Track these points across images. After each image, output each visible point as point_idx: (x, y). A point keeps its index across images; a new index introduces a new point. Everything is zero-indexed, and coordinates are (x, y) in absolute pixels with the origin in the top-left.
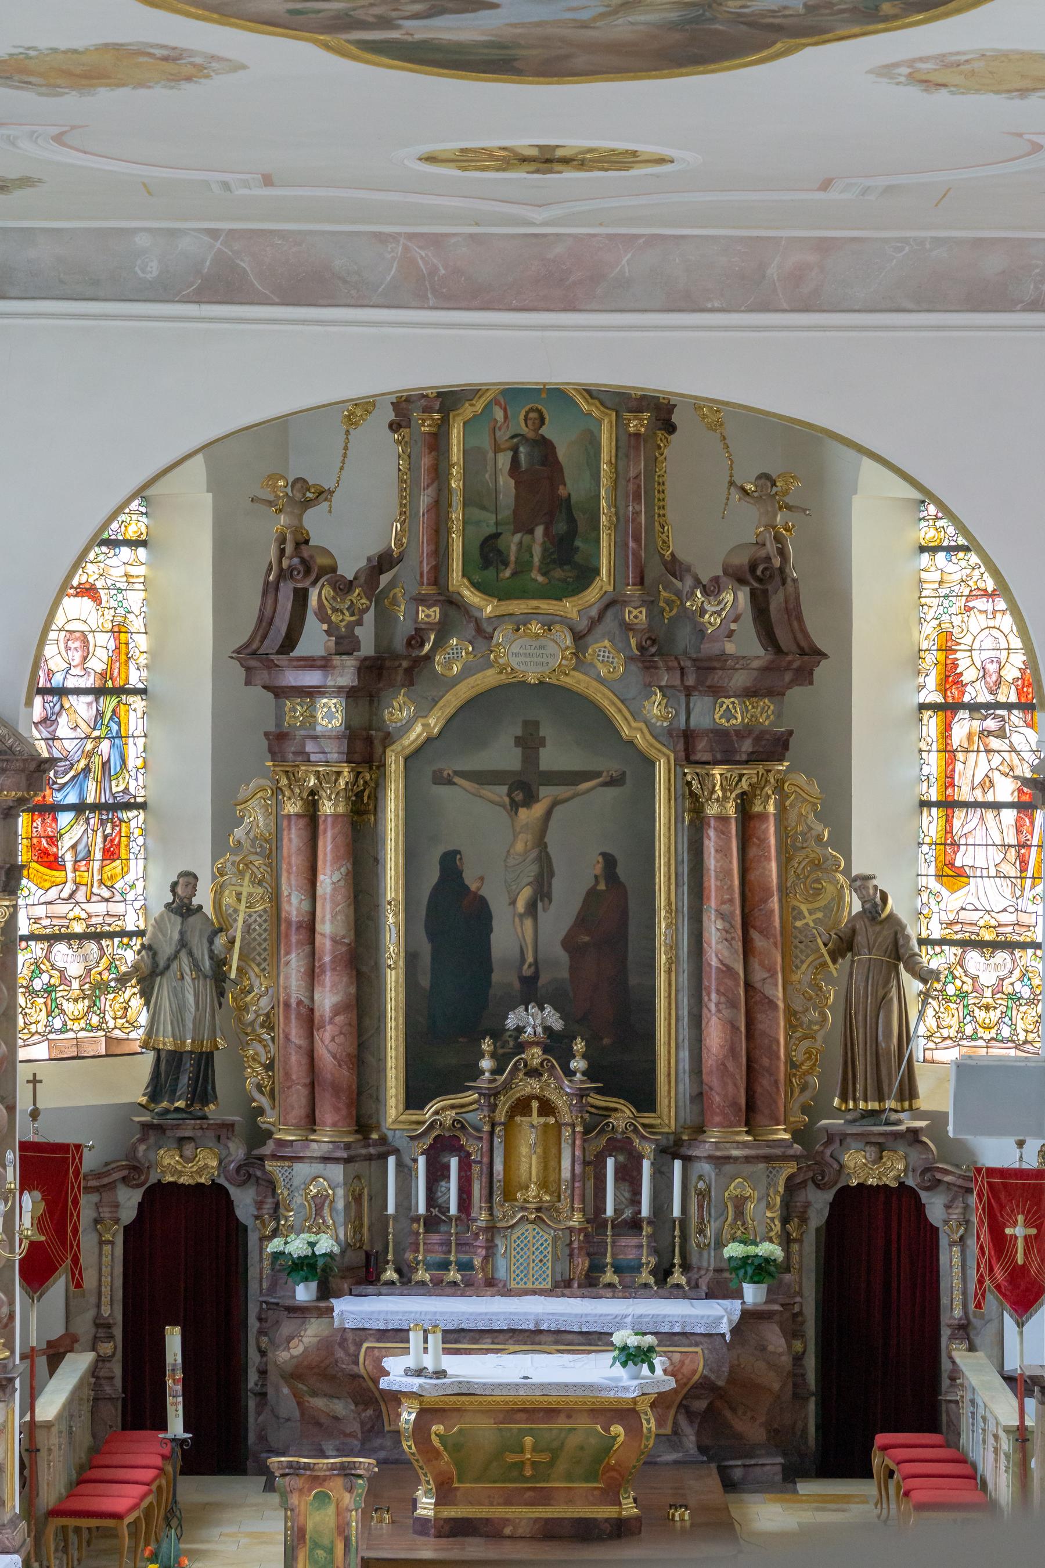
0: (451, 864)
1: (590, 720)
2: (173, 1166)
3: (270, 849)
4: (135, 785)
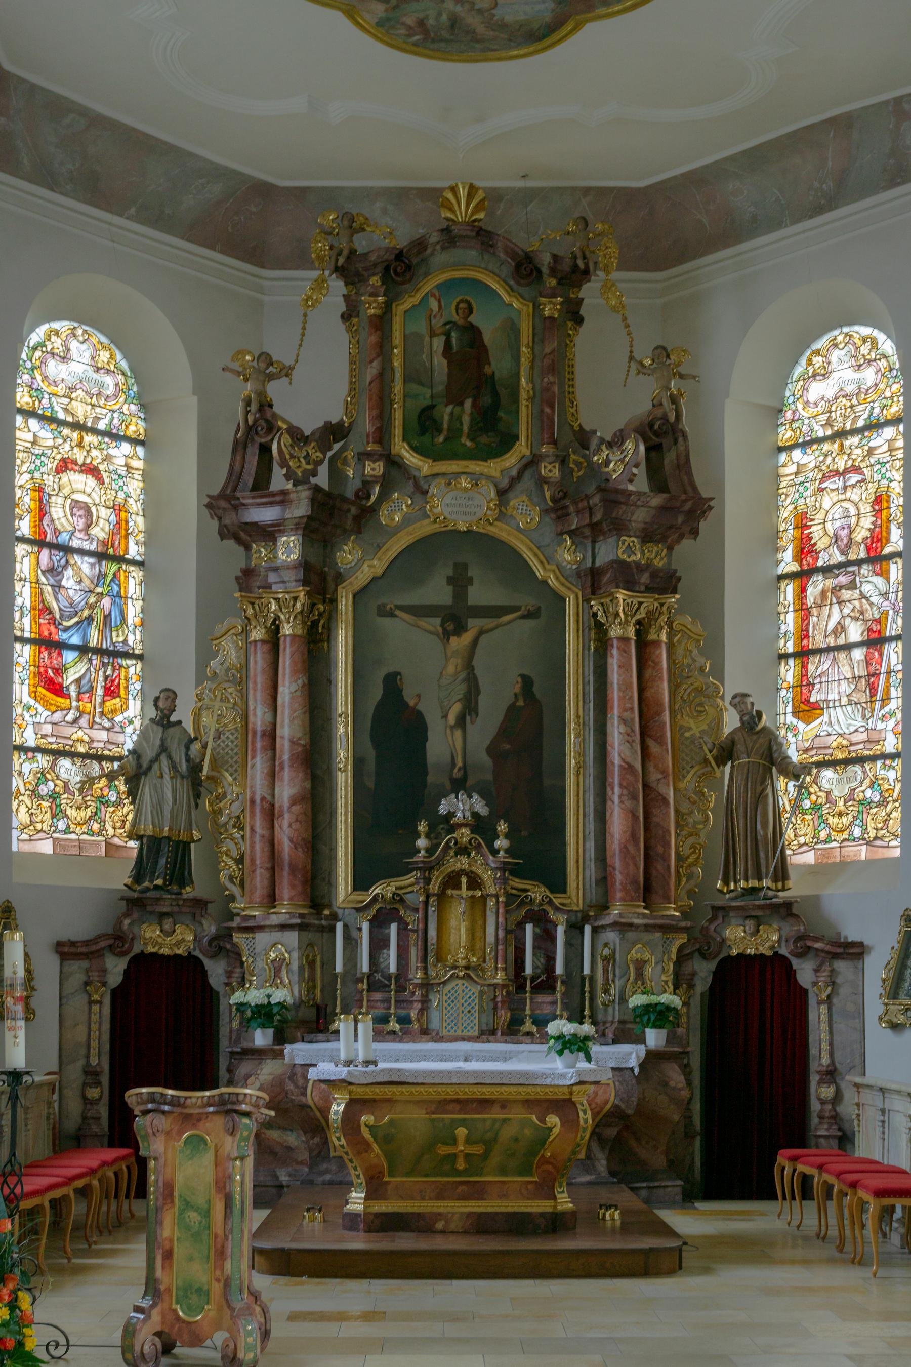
0: (392, 682)
1: (512, 566)
3: (240, 677)
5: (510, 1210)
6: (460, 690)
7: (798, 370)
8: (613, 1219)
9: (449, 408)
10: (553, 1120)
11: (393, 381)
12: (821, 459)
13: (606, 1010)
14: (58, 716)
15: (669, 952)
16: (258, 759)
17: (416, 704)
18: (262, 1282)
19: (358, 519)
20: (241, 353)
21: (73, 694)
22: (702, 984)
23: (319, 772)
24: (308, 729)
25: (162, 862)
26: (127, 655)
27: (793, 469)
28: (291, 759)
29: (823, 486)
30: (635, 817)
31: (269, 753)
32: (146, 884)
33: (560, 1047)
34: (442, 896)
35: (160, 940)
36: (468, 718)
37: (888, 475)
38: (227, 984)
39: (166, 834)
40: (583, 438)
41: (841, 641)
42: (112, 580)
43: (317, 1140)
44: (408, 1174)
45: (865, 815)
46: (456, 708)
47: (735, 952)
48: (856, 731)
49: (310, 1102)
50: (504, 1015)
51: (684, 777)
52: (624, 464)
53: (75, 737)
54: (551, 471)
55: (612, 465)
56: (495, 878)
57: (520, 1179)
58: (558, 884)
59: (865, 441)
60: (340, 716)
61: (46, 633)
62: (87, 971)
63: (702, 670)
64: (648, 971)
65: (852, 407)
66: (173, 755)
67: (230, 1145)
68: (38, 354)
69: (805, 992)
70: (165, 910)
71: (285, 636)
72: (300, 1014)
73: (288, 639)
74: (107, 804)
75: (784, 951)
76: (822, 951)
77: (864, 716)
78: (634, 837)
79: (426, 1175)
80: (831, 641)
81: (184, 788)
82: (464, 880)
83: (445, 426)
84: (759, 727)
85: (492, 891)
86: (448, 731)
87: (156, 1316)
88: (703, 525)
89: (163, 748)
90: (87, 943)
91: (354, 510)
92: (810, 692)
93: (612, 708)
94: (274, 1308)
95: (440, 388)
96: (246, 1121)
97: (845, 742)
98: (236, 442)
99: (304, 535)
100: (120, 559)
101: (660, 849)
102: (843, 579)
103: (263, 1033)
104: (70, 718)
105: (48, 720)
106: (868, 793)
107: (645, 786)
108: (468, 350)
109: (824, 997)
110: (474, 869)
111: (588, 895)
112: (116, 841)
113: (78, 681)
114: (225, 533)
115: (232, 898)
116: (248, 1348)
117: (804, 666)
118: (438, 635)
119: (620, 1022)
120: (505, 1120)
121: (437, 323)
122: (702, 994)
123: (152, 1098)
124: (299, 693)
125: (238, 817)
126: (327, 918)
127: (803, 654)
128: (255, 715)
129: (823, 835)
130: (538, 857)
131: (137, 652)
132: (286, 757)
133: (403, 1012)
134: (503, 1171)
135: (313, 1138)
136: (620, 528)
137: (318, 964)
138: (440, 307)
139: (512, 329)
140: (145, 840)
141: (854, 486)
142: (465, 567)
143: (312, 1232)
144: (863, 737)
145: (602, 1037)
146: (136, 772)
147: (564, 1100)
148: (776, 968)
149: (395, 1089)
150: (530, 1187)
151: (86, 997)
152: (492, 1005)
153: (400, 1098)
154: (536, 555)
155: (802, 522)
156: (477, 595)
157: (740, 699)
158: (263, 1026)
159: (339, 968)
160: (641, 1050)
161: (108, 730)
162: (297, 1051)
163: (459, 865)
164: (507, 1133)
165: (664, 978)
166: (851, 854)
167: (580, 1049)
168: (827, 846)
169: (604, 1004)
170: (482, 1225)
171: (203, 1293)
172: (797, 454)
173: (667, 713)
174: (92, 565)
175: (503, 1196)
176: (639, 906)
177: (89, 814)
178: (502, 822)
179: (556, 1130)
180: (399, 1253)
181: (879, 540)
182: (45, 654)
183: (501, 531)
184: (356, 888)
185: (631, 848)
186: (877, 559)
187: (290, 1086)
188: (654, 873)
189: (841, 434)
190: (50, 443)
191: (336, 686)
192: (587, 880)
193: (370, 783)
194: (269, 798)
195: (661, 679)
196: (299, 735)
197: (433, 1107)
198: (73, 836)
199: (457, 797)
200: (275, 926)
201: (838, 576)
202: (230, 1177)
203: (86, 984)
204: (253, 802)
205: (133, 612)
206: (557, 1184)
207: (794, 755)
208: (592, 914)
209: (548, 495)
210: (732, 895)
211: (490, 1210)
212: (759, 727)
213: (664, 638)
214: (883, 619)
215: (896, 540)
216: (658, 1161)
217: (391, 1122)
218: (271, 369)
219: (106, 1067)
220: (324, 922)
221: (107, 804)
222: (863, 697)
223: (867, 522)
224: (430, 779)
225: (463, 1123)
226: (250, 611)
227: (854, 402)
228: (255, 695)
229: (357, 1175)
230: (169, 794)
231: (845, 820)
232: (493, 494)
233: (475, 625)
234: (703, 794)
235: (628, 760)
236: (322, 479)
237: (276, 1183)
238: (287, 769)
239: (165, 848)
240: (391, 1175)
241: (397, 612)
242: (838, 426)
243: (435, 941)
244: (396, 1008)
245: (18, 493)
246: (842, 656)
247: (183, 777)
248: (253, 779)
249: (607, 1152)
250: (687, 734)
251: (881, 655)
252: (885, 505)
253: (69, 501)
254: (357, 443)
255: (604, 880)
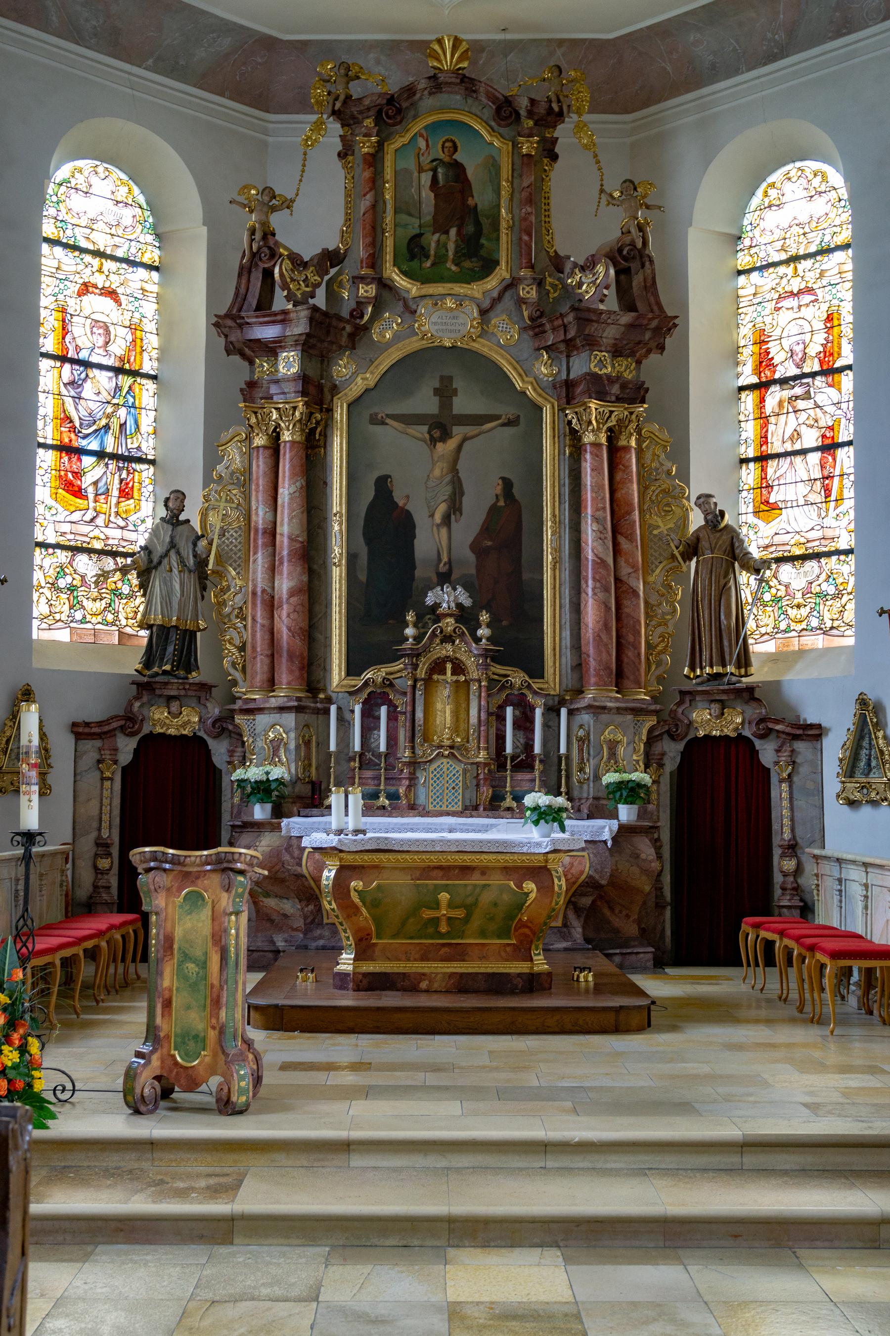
0: (383, 485)
2: (162, 720)
4: (148, 447)
5: (489, 970)
6: (446, 491)
7: (755, 202)
8: (587, 981)
9: (437, 235)
10: (530, 886)
11: (384, 212)
12: (777, 281)
13: (581, 787)
14: (76, 516)
15: (640, 734)
16: (260, 554)
17: (405, 504)
18: (257, 1035)
19: (352, 336)
20: (247, 187)
21: (91, 497)
22: (671, 764)
23: (315, 567)
24: (305, 526)
25: (170, 649)
26: (140, 460)
27: (752, 290)
28: (289, 555)
29: (779, 305)
30: (607, 608)
31: (270, 549)
32: (156, 669)
33: (535, 818)
34: (428, 681)
35: (167, 721)
36: (453, 517)
37: (839, 295)
38: (229, 763)
39: (174, 624)
40: (558, 263)
41: (797, 446)
42: (128, 392)
43: (311, 907)
44: (394, 936)
45: (822, 607)
46: (442, 508)
47: (701, 733)
48: (813, 529)
49: (305, 872)
50: (487, 792)
51: (653, 571)
52: (595, 285)
53: (91, 535)
54: (528, 292)
55: (584, 287)
56: (478, 665)
57: (498, 941)
58: (536, 670)
59: (817, 265)
60: (335, 515)
61: (66, 440)
62: (100, 749)
63: (669, 473)
64: (621, 751)
65: (804, 234)
66: (182, 551)
67: (225, 901)
68: (63, 189)
69: (766, 772)
70: (173, 693)
71: (285, 442)
72: (296, 790)
73: (288, 445)
74: (120, 596)
75: (747, 733)
76: (783, 732)
77: (819, 515)
78: (606, 626)
79: (411, 938)
80: (789, 447)
81: (192, 581)
82: (449, 666)
83: (432, 253)
84: (722, 525)
85: (475, 675)
86: (435, 528)
87: (155, 1061)
88: (668, 341)
89: (173, 545)
90: (100, 724)
91: (349, 328)
92: (769, 493)
93: (586, 508)
94: (267, 1059)
95: (428, 218)
96: (241, 878)
97: (803, 540)
98: (242, 268)
99: (303, 351)
100: (135, 373)
101: (631, 638)
102: (798, 391)
103: (263, 809)
104: (88, 517)
105: (68, 519)
106: (824, 586)
107: (617, 580)
108: (453, 186)
109: (785, 775)
110: (458, 655)
111: (564, 680)
112: (128, 630)
113: (95, 483)
114: (231, 349)
115: (234, 683)
116: (241, 1092)
117: (764, 470)
118: (424, 441)
119: (594, 798)
120: (485, 886)
121: (425, 160)
122: (671, 773)
123: (154, 857)
124: (297, 494)
125: (241, 608)
126: (322, 701)
127: (762, 459)
128: (257, 514)
129: (783, 626)
130: (518, 645)
131: (149, 457)
132: (285, 553)
133: (392, 789)
134: (483, 934)
135: (307, 906)
136: (592, 343)
137: (314, 744)
138: (428, 146)
139: (493, 166)
140: (155, 629)
141: (807, 305)
142: (450, 379)
143: (305, 990)
144: (819, 534)
145: (578, 814)
146: (147, 566)
147: (540, 868)
148: (740, 748)
149: (382, 856)
150: (508, 949)
151: (98, 773)
152: (475, 783)
153: (387, 865)
154: (515, 369)
155: (761, 340)
156: (462, 405)
157: (704, 500)
158: (262, 801)
159: (333, 747)
160: (614, 825)
161: (122, 528)
162: (293, 825)
163: (444, 652)
164: (486, 898)
165: (635, 758)
166: (809, 643)
167: (554, 820)
168: (787, 635)
169: (579, 782)
170: (463, 985)
171: (200, 1040)
172: (755, 275)
173: (637, 512)
174: (110, 378)
175: (483, 958)
176: (611, 691)
177: (104, 605)
178: (484, 612)
179: (533, 896)
180: (386, 1009)
181: (831, 354)
182: (66, 459)
183: (482, 347)
184: (348, 674)
185: (604, 637)
186: (829, 372)
187: (286, 857)
188: (626, 660)
189: (795, 259)
190: (73, 268)
191: (332, 488)
192: (563, 666)
193: (363, 577)
194: (269, 590)
195: (631, 481)
196: (297, 532)
197: (418, 873)
198: (89, 626)
199: (442, 590)
200: (274, 708)
201: (793, 387)
202: (226, 931)
203: (99, 762)
204: (254, 594)
205: (147, 421)
206: (533, 947)
207: (756, 553)
208: (568, 698)
209: (526, 314)
210: (698, 680)
211: (470, 970)
212: (722, 525)
213: (633, 443)
214: (836, 427)
215: (847, 357)
216: (631, 929)
217: (379, 887)
218: (274, 201)
219: (116, 839)
220: (319, 705)
221: (120, 596)
222: (818, 498)
223: (820, 338)
224: (418, 573)
225: (446, 888)
226: (253, 420)
227: (807, 230)
228: (257, 496)
229: (347, 938)
230: (177, 587)
231: (804, 611)
232: (476, 314)
233: (458, 432)
234: (671, 587)
235: (601, 555)
236: (320, 300)
237: (273, 948)
238: (286, 564)
239: (173, 637)
240: (379, 936)
241: (388, 421)
242: (793, 252)
243: (421, 722)
244: (386, 785)
245: (43, 313)
246: (798, 459)
247: (190, 571)
248: (255, 572)
249: (582, 919)
250: (655, 532)
251: (834, 460)
252: (836, 322)
253: (89, 321)
254: (351, 268)
255: (579, 667)
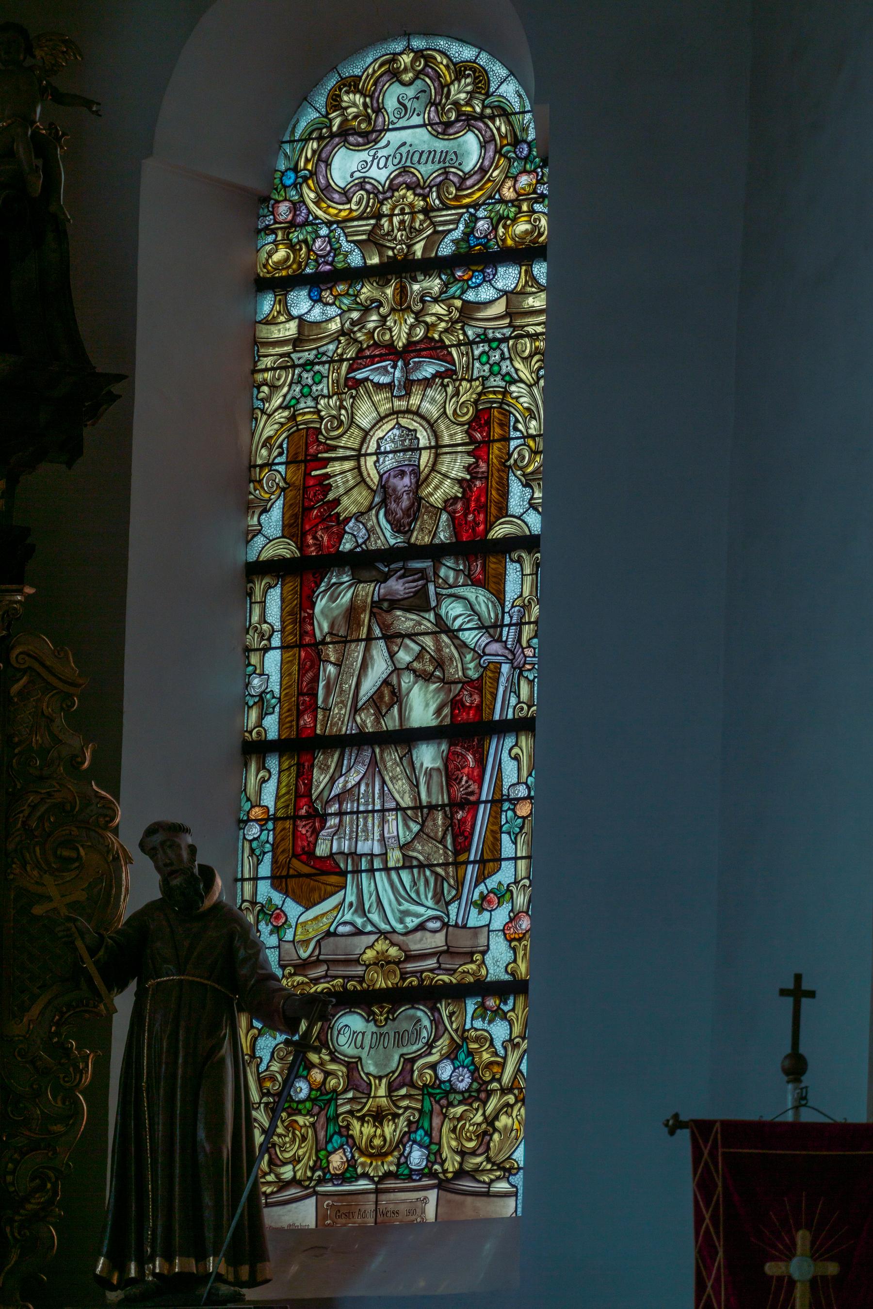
27: (291, 329)
29: (360, 375)
41: (391, 723)
45: (436, 1121)
48: (421, 927)
77: (438, 897)
80: (367, 721)
92: (316, 833)
97: (393, 951)
102: (397, 586)
106: (446, 1071)
117: (304, 775)
127: (302, 747)
144: (438, 941)
166: (403, 1208)
201: (385, 578)
210: (134, 1290)
214: (488, 683)
223: (455, 466)
246: (391, 757)
251: (481, 763)
